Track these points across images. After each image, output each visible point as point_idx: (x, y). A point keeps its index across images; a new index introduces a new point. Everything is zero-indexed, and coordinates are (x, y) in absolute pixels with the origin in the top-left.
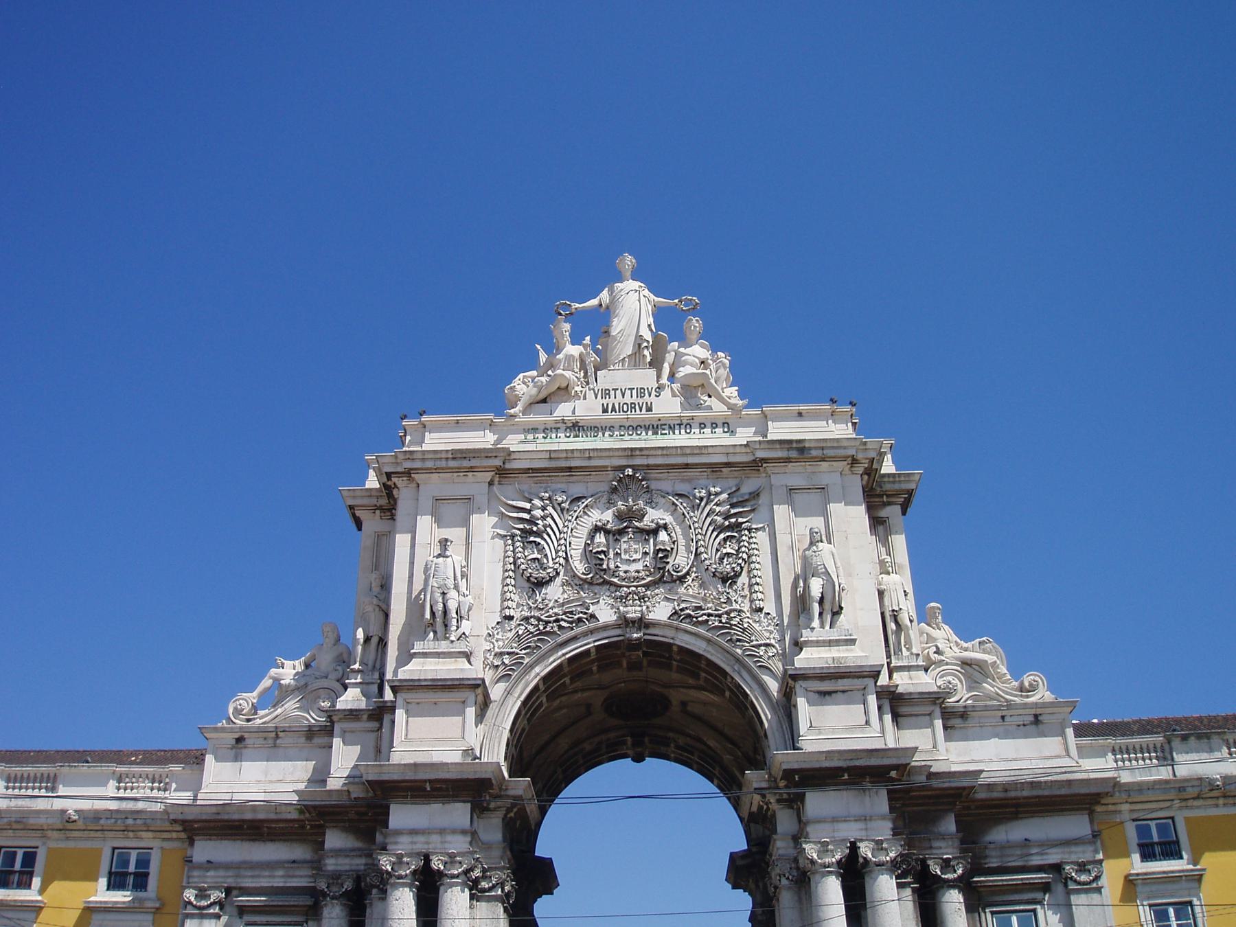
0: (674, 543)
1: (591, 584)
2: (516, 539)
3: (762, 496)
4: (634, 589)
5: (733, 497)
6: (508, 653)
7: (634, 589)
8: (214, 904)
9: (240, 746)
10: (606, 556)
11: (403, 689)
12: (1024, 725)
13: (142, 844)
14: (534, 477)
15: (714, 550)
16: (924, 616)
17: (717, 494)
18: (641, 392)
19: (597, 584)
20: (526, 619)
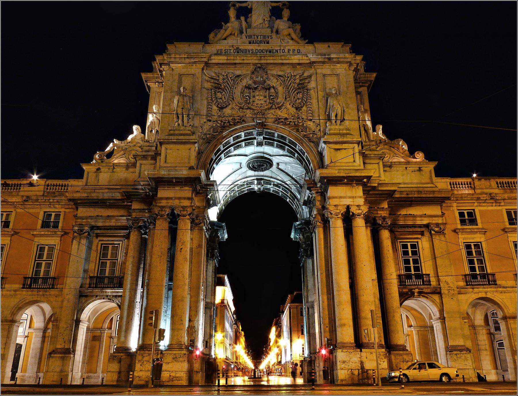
0: (277, 93)
1: (242, 109)
2: (213, 90)
3: (312, 77)
4: (260, 111)
5: (301, 78)
6: (209, 134)
7: (260, 111)
8: (85, 233)
9: (98, 172)
10: (249, 98)
11: (164, 143)
12: (415, 171)
13: (57, 210)
14: (220, 67)
15: (293, 96)
16: (374, 130)
17: (294, 76)
18: (264, 37)
19: (245, 109)
20: (217, 121)
